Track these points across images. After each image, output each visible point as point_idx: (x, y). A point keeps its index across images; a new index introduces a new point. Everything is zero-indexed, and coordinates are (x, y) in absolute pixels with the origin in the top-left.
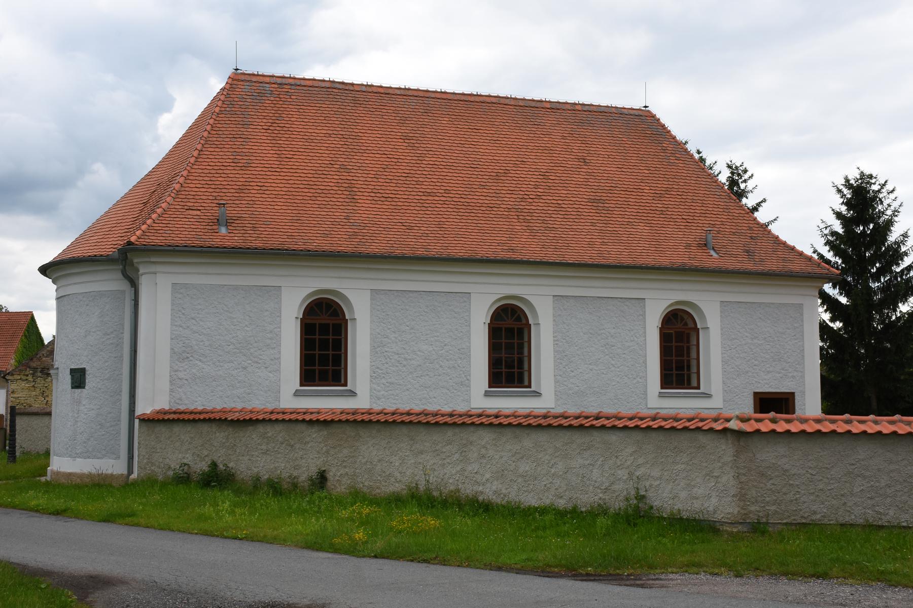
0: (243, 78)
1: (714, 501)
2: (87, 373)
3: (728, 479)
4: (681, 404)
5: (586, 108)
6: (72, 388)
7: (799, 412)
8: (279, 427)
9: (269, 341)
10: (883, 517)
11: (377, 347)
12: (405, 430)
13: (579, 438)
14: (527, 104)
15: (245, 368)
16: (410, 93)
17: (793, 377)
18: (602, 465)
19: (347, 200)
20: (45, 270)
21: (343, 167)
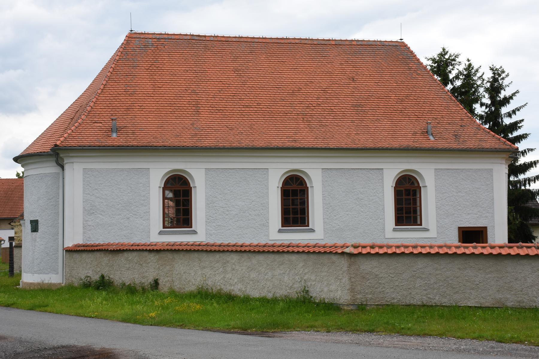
0: (135, 36)
1: (339, 292)
2: (39, 223)
3: (345, 280)
4: (409, 236)
5: (360, 43)
6: (32, 232)
7: (490, 241)
8: (134, 254)
9: (142, 202)
10: (432, 300)
11: (209, 204)
12: (196, 255)
13: (277, 257)
14: (319, 42)
15: (128, 218)
16: (242, 40)
17: (486, 217)
18: (289, 274)
19: (194, 113)
20: (16, 159)
21: (194, 92)
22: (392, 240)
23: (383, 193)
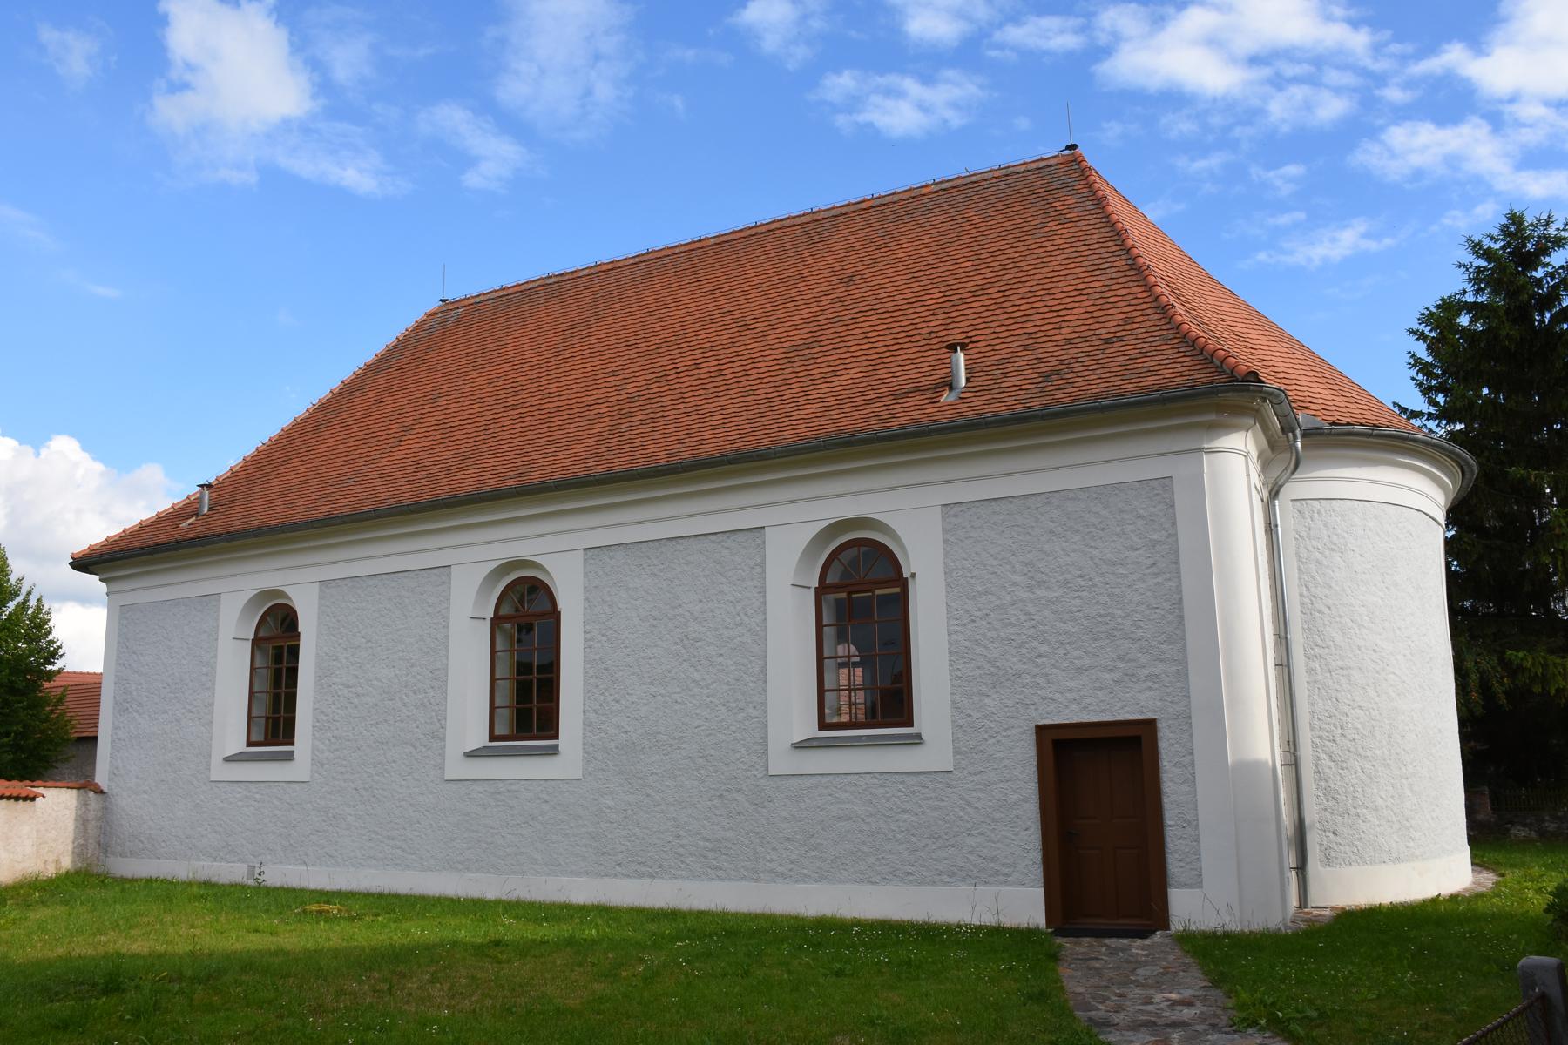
5: (943, 186)
17: (1149, 676)
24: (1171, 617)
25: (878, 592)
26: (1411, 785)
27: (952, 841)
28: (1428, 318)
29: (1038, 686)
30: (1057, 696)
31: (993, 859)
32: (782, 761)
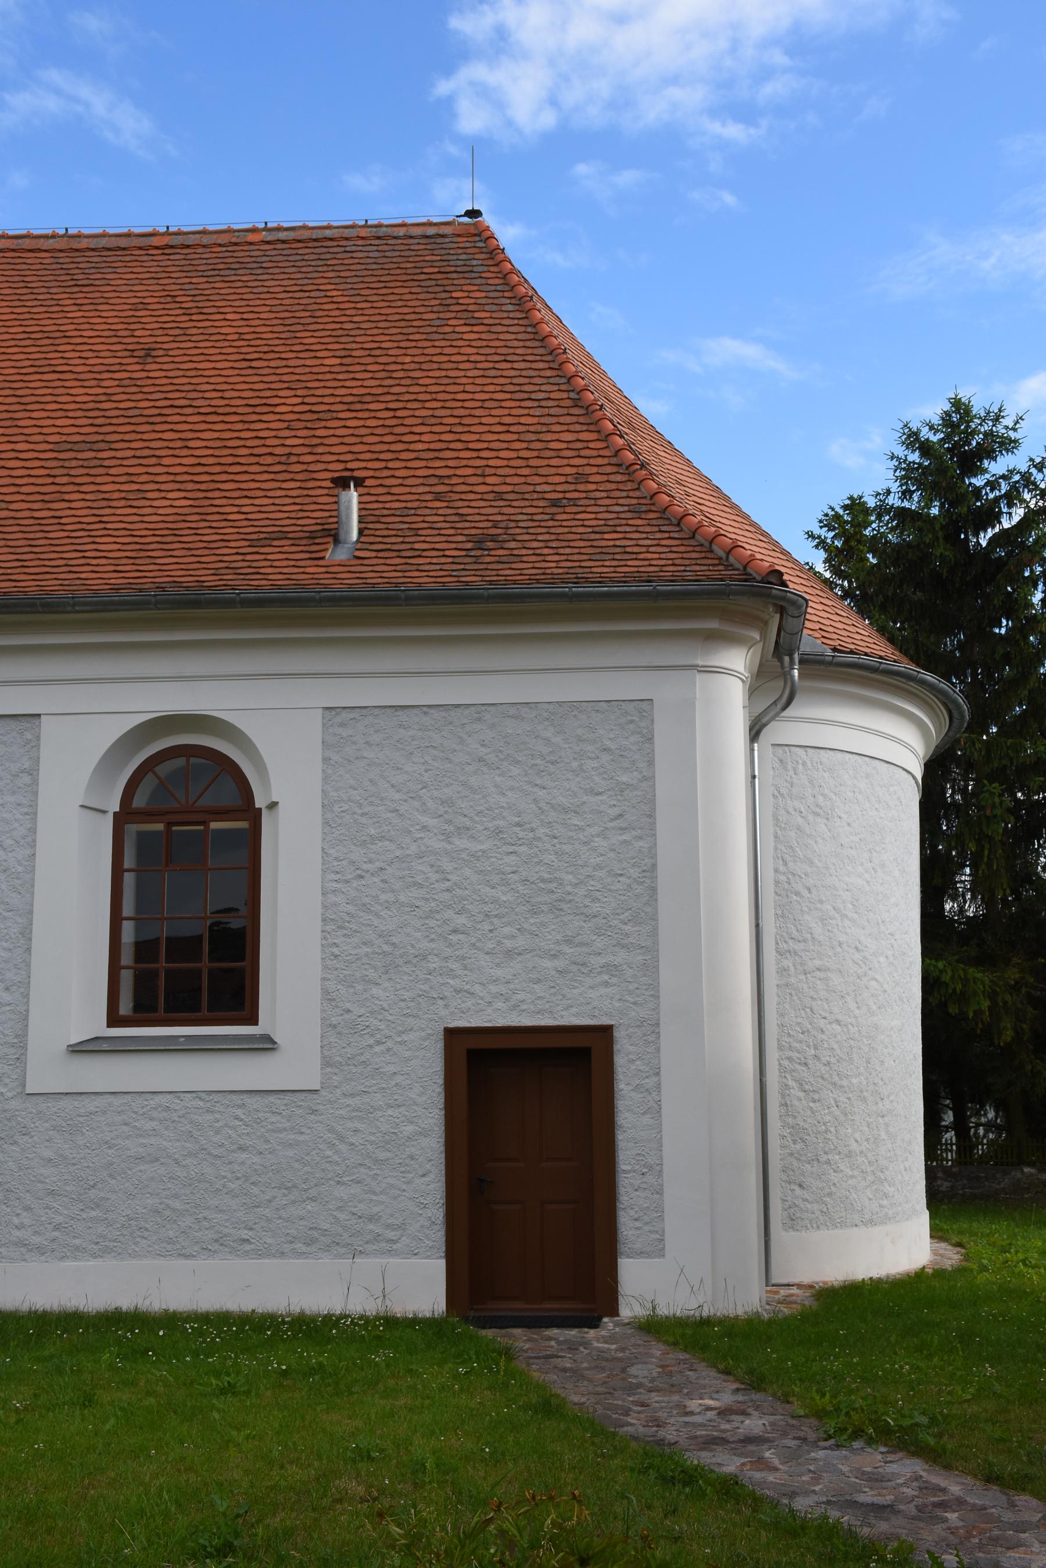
5: (282, 235)
17: (608, 968)
22: (65, 1103)
23: (33, 845)
24: (639, 889)
25: (214, 825)
26: (887, 1125)
27: (313, 1192)
28: (832, 521)
29: (451, 973)
30: (477, 989)
31: (371, 1219)
32: (48, 1070)
